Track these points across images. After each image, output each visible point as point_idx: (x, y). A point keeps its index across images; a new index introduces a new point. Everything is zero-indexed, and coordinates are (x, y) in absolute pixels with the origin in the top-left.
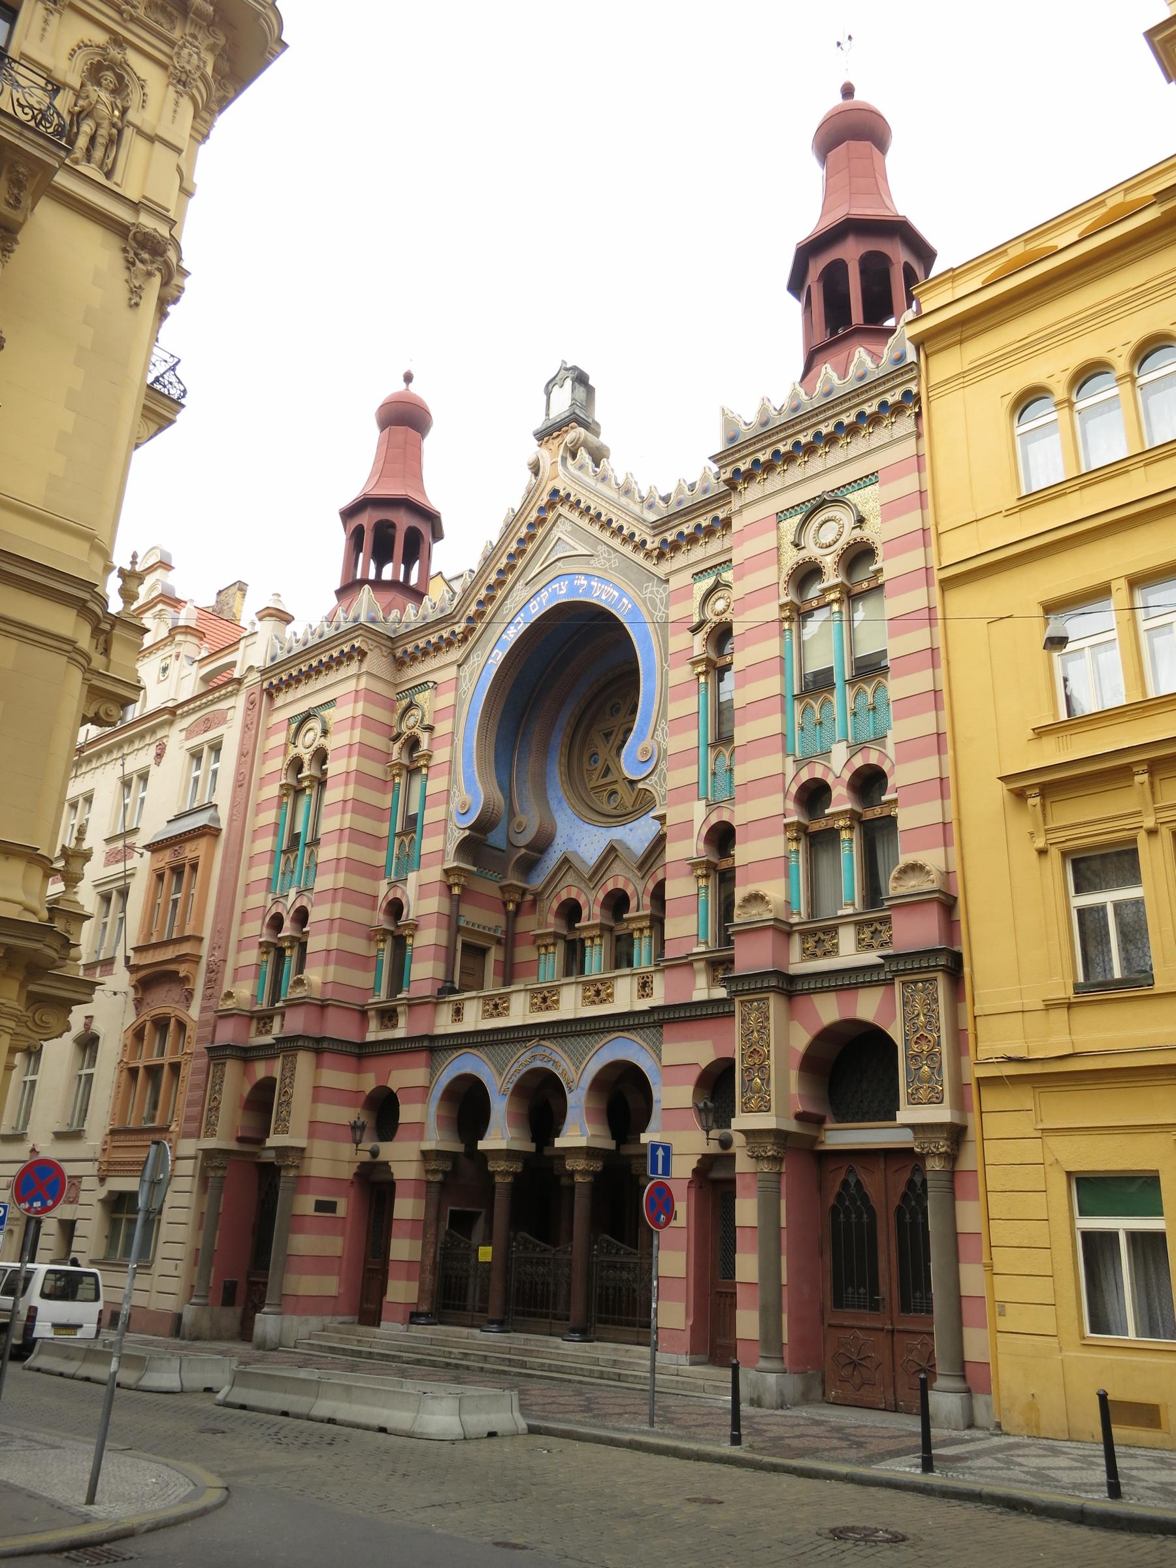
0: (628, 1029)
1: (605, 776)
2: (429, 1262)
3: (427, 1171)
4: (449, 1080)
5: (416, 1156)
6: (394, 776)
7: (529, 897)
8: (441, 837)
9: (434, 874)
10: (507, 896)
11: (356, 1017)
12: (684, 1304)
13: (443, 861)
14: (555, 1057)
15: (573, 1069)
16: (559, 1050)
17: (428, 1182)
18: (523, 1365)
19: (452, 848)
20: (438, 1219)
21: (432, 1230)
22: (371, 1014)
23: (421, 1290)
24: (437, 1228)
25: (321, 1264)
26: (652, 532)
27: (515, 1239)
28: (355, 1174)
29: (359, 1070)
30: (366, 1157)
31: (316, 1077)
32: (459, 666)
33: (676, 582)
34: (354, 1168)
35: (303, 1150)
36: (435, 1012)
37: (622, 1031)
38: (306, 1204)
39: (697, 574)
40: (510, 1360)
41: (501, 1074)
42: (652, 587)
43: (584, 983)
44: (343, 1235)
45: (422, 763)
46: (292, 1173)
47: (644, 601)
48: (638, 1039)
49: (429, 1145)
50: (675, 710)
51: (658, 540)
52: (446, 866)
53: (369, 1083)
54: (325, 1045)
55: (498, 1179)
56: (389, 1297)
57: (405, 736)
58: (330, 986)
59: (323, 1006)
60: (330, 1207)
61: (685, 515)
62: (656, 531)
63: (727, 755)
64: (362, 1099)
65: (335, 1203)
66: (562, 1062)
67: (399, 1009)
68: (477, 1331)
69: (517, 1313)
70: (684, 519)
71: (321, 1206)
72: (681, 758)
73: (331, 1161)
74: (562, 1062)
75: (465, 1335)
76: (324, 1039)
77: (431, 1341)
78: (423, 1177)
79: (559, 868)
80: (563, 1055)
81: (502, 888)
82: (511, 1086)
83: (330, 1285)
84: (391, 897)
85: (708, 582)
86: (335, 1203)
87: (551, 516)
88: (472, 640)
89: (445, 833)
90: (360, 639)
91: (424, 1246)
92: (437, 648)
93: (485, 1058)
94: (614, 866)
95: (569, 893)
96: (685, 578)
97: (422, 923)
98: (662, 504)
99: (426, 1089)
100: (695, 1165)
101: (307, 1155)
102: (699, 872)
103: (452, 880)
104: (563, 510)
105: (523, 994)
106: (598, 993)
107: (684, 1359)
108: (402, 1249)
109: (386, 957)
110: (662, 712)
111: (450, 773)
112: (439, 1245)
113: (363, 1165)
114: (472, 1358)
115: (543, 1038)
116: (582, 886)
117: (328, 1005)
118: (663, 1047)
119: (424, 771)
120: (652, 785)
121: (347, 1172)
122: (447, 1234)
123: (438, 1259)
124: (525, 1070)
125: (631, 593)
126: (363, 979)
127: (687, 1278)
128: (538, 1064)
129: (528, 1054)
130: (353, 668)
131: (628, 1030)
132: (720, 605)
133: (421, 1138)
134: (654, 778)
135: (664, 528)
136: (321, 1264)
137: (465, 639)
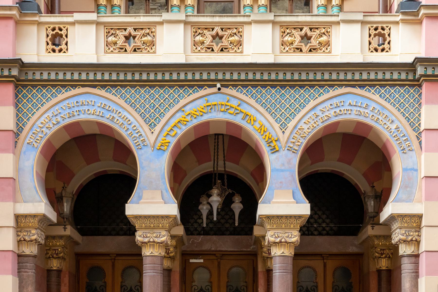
0: (362, 84)
5: (12, 222)
14: (245, 108)
15: (277, 126)
16: (252, 102)
36: (17, 35)
37: (353, 86)
41: (152, 126)
43: (282, 25)
48: (376, 97)
49: (24, 208)
55: (146, 252)
66: (259, 116)
74: (259, 116)
82: (173, 141)
93: (122, 102)
106: (306, 38)
124: (196, 122)
128: (216, 116)
129: (201, 103)
131: (361, 87)
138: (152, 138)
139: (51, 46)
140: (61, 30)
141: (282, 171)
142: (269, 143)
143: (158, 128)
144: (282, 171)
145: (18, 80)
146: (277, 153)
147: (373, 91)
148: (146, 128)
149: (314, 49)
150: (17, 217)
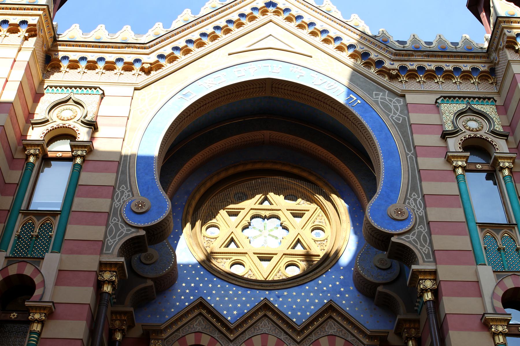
1: (227, 246)
6: (28, 156)
7: (136, 333)
8: (103, 228)
9: (90, 262)
10: (117, 322)
13: (101, 253)
19: (115, 243)
26: (393, 57)
32: (136, 89)
33: (410, 98)
39: (445, 97)
42: (383, 96)
45: (79, 153)
47: (377, 102)
50: (429, 187)
51: (397, 65)
52: (105, 259)
57: (55, 125)
61: (428, 56)
62: (397, 58)
63: (499, 237)
70: (426, 59)
72: (450, 228)
79: (188, 313)
81: (112, 313)
84: (13, 270)
85: (461, 106)
87: (261, 19)
88: (155, 75)
89: (107, 225)
90: (38, 18)
92: (110, 67)
94: (260, 324)
95: (198, 339)
96: (431, 99)
97: (59, 310)
98: (397, 44)
102: (500, 329)
103: (107, 276)
104: (280, 19)
110: (414, 186)
111: (117, 173)
116: (216, 335)
119: (78, 161)
120: (410, 242)
125: (360, 92)
130: (15, 39)
132: (473, 125)
134: (411, 237)
135: (406, 58)
137: (147, 72)
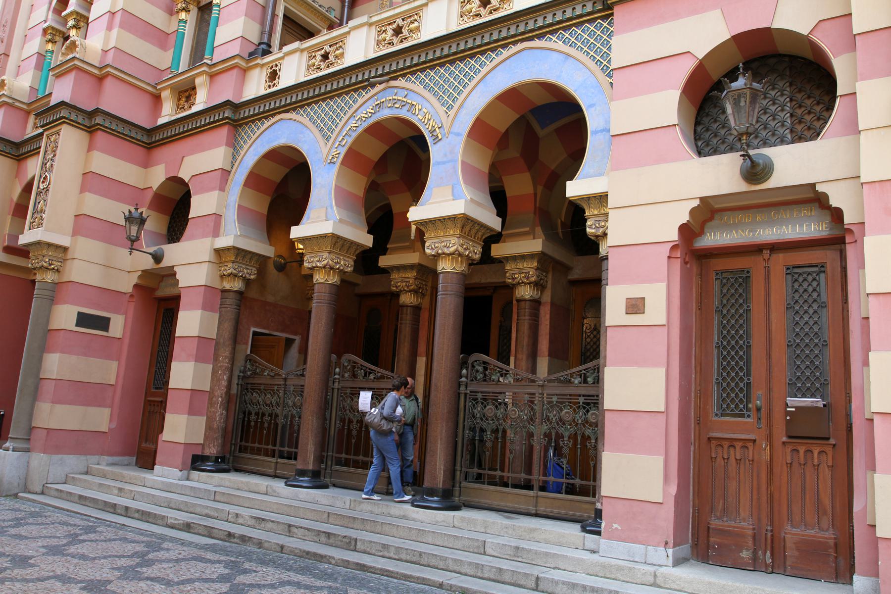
2: (220, 393)
3: (222, 277)
4: (256, 158)
11: (147, 100)
12: (661, 459)
16: (420, 89)
17: (224, 291)
18: (351, 544)
20: (236, 339)
21: (225, 352)
22: (166, 94)
23: (209, 427)
24: (234, 349)
25: (83, 393)
27: (338, 364)
28: (136, 286)
29: (146, 164)
30: (148, 263)
31: (87, 161)
34: (134, 279)
35: (65, 249)
37: (531, 39)
38: (65, 316)
40: (328, 535)
44: (118, 359)
46: (49, 277)
48: (559, 46)
53: (157, 176)
54: (99, 120)
55: (319, 278)
56: (167, 435)
58: (111, 53)
59: (100, 77)
60: (103, 323)
64: (149, 196)
65: (108, 320)
66: (425, 104)
67: (198, 81)
68: (279, 485)
69: (339, 462)
71: (84, 320)
73: (101, 267)
75: (264, 489)
76: (97, 111)
77: (215, 497)
78: (217, 284)
80: (426, 94)
82: (343, 151)
83: (100, 419)
86: (108, 320)
91: (214, 372)
99: (225, 173)
100: (685, 218)
101: (69, 256)
105: (365, 29)
107: (662, 555)
108: (184, 374)
109: (189, 31)
112: (236, 373)
113: (145, 273)
114: (270, 525)
115: (394, 75)
117: (108, 74)
118: (614, 41)
121: (127, 284)
122: (248, 359)
123: (234, 391)
124: (365, 125)
126: (161, 59)
127: (666, 412)
128: (385, 113)
129: (372, 103)
131: (540, 37)
133: (216, 233)
136: (83, 393)
138: (325, 151)
139: (268, 84)
140: (276, 66)
141: (444, 163)
142: (432, 132)
143: (331, 141)
144: (444, 163)
145: (235, 121)
146: (440, 143)
147: (554, 39)
148: (322, 142)
149: (495, 10)
150: (218, 252)
